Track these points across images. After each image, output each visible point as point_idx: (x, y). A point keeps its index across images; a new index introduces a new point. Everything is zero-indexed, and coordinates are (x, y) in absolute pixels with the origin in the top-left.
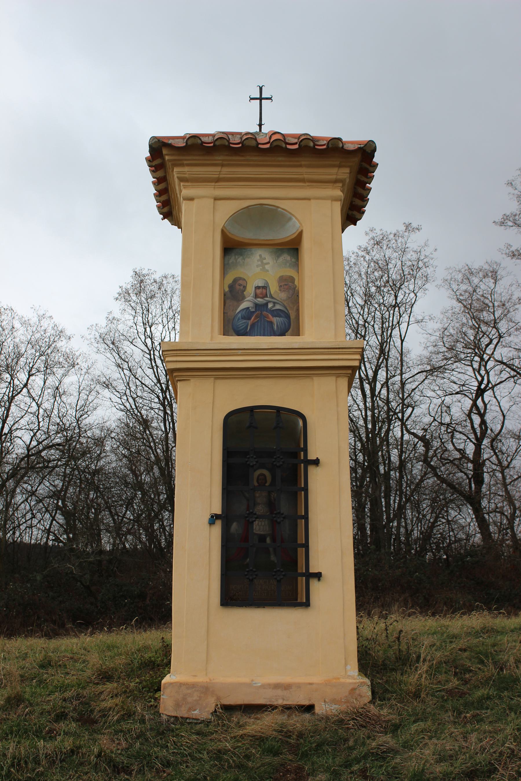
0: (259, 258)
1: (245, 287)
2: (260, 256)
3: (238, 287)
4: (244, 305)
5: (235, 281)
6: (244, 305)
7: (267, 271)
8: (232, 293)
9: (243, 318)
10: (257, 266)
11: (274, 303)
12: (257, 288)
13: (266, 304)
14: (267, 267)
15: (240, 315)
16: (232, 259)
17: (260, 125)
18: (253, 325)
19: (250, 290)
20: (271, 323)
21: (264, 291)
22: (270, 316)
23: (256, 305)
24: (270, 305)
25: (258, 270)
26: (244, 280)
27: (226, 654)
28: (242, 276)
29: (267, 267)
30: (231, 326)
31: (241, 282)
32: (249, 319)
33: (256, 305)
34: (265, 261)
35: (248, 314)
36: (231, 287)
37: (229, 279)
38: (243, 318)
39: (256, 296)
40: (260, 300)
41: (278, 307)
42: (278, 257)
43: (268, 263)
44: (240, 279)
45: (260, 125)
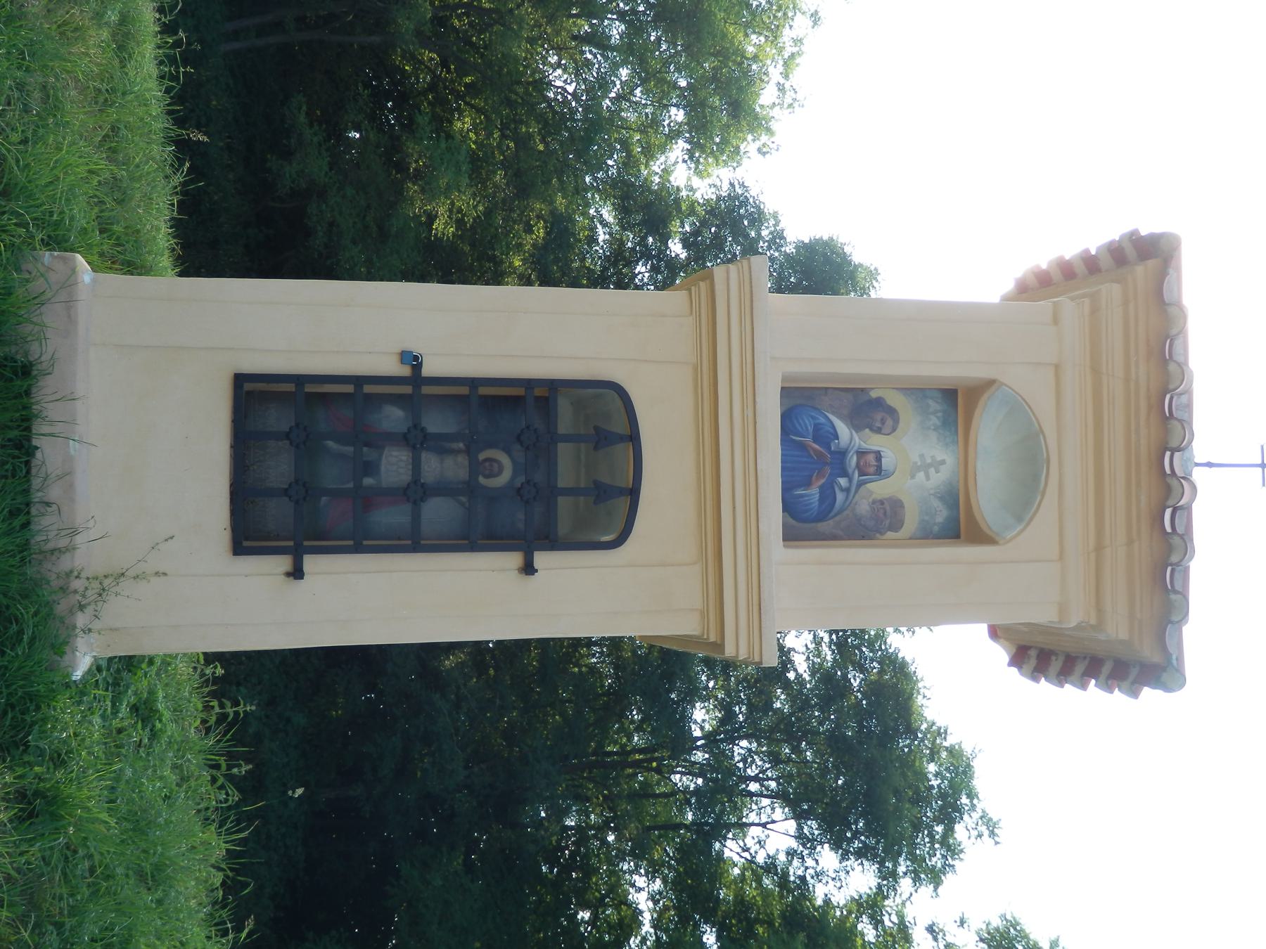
0: (939, 459)
1: (879, 431)
2: (943, 462)
3: (879, 416)
4: (843, 429)
5: (892, 412)
6: (843, 429)
7: (913, 477)
8: (867, 407)
9: (817, 428)
10: (922, 456)
11: (847, 490)
12: (878, 456)
13: (845, 474)
14: (921, 475)
15: (822, 420)
16: (933, 405)
18: (802, 447)
19: (874, 442)
20: (808, 484)
21: (872, 470)
22: (823, 481)
23: (843, 454)
24: (843, 481)
25: (915, 458)
26: (894, 430)
27: (152, 367)
28: (901, 425)
29: (921, 475)
30: (800, 402)
31: (889, 422)
32: (816, 439)
33: (843, 454)
34: (932, 470)
35: (825, 436)
36: (879, 403)
37: (895, 400)
38: (817, 428)
39: (861, 453)
40: (853, 460)
41: (840, 497)
42: (941, 499)
43: (928, 478)
44: (896, 421)
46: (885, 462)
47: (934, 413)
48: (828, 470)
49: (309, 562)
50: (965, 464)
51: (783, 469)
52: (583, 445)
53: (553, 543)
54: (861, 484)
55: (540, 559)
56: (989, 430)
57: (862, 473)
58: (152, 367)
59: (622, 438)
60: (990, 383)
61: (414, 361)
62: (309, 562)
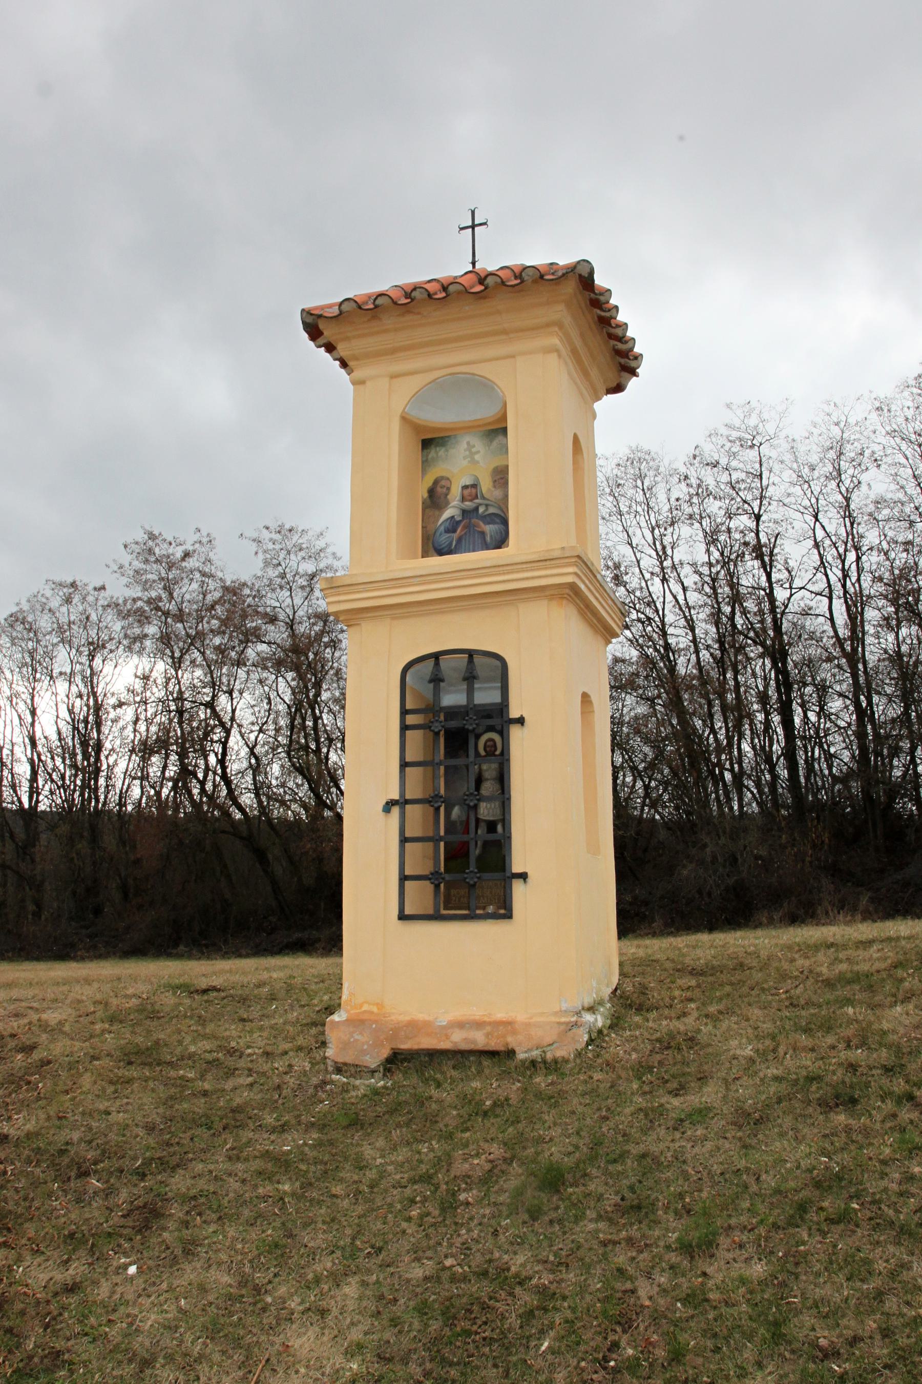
0: (466, 446)
1: (449, 489)
2: (468, 443)
3: (439, 490)
4: (447, 514)
5: (436, 482)
6: (447, 514)
7: (478, 462)
8: (435, 498)
9: (447, 531)
10: (465, 458)
11: (487, 506)
12: (465, 487)
13: (477, 509)
14: (477, 457)
15: (442, 528)
16: (432, 453)
17: (474, 263)
18: (460, 540)
19: (456, 492)
20: (483, 533)
21: (474, 490)
22: (481, 523)
23: (464, 512)
24: (481, 510)
25: (465, 463)
26: (448, 479)
27: (399, 972)
28: (444, 474)
29: (477, 457)
30: (434, 546)
31: (443, 483)
32: (454, 531)
33: (464, 512)
34: (474, 450)
35: (452, 525)
36: (431, 492)
37: (429, 481)
38: (447, 531)
39: (463, 499)
40: (468, 505)
41: (491, 510)
42: (491, 441)
43: (478, 452)
44: (442, 478)
45: (474, 263)
46: (468, 482)
47: (437, 453)
48: (474, 521)
49: (516, 868)
50: (468, 428)
51: (474, 551)
52: (476, 686)
53: (504, 706)
54: (483, 498)
55: (514, 713)
56: (437, 416)
57: (476, 497)
58: (399, 972)
59: (437, 663)
60: (404, 419)
61: (389, 806)
62: (516, 868)
